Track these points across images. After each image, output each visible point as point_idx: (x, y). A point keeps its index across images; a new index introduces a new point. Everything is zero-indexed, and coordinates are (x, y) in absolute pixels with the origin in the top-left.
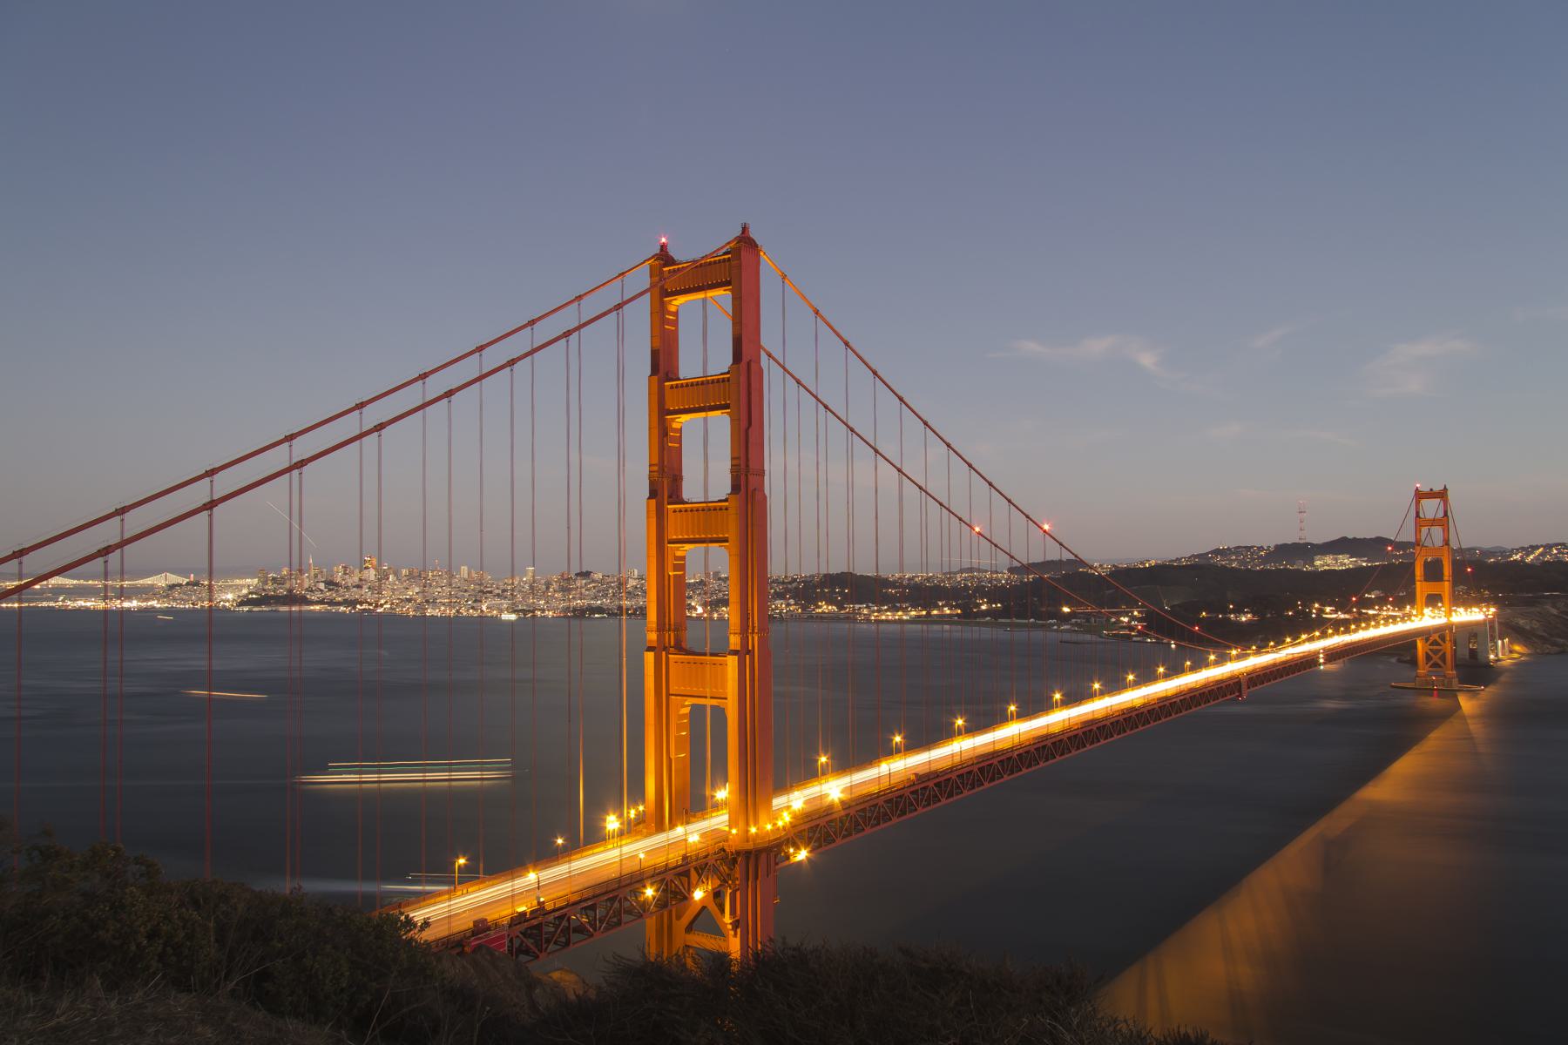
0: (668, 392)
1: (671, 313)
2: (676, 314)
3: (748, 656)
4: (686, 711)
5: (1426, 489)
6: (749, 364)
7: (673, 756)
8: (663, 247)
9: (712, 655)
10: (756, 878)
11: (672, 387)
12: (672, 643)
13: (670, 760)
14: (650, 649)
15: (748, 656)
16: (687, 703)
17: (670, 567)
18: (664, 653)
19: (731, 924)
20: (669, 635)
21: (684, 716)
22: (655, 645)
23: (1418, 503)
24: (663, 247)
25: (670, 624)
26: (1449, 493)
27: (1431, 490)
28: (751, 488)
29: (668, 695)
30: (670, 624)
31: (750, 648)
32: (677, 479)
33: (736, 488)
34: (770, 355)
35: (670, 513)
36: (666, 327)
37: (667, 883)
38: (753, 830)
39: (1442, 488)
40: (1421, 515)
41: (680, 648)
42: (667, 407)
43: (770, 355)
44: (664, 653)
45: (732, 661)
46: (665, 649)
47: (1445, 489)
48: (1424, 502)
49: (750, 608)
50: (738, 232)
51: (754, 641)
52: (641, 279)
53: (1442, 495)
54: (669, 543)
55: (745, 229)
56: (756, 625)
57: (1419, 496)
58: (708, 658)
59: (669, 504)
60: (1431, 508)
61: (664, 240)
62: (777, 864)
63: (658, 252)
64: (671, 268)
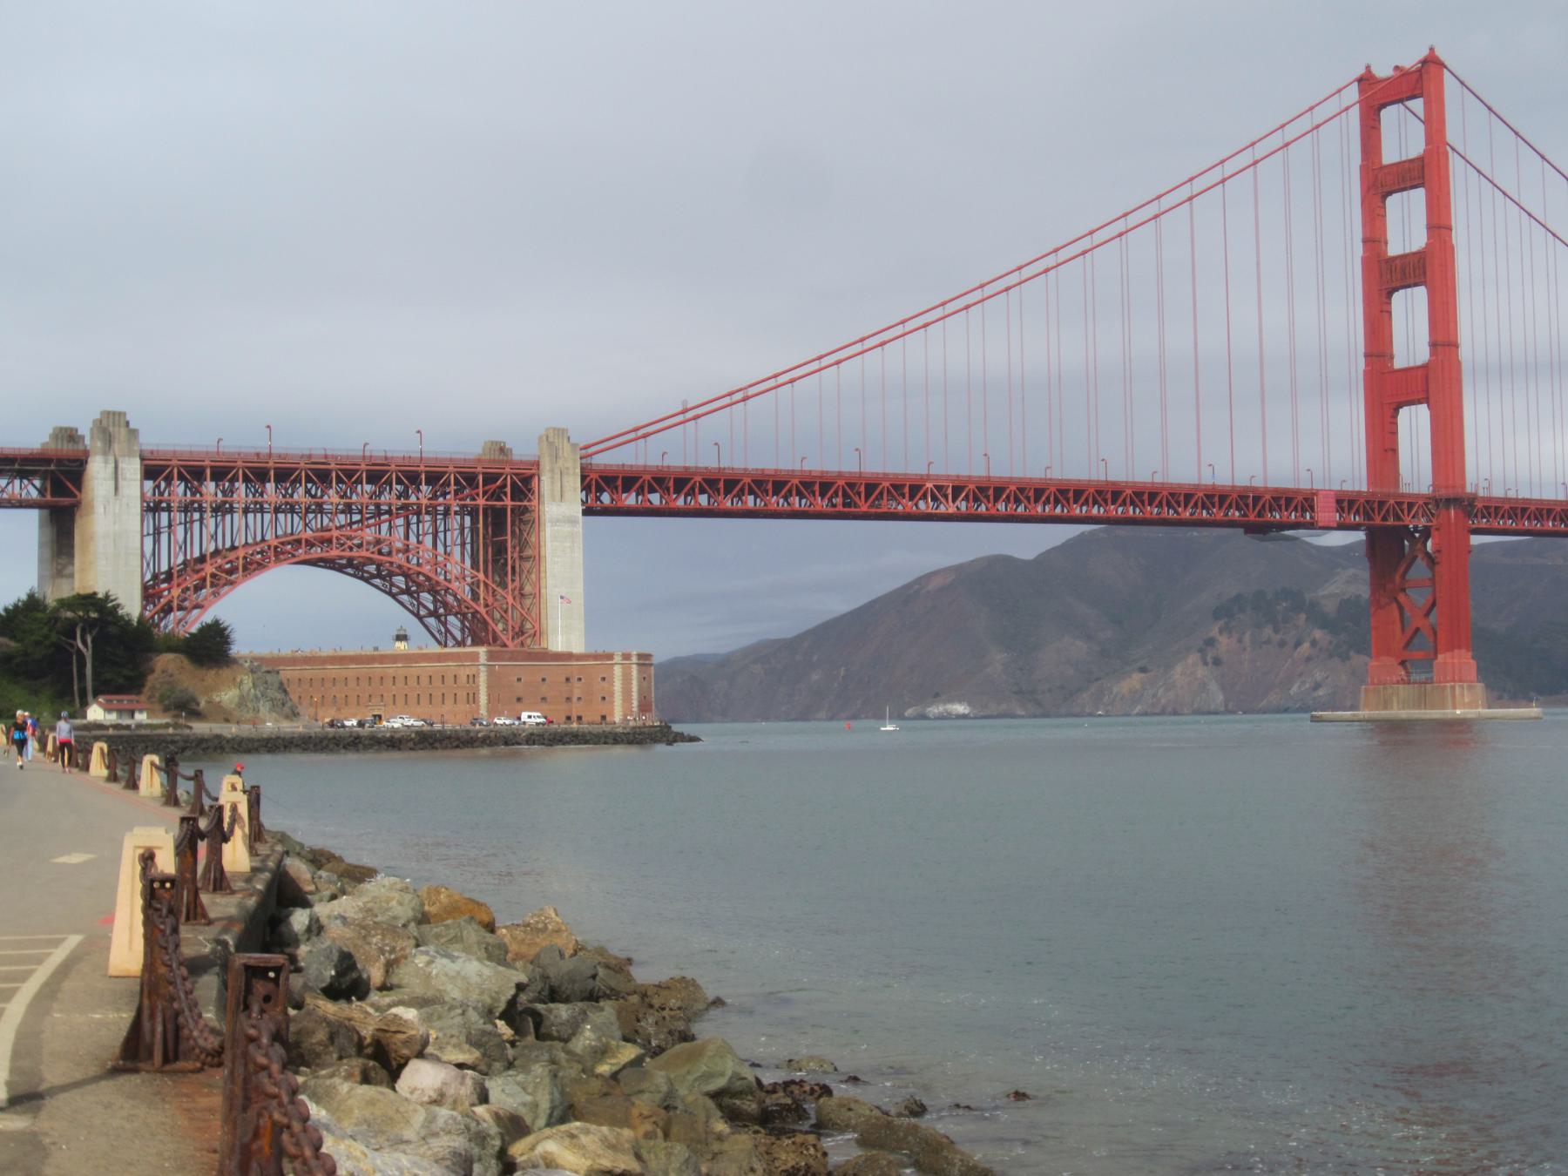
24: (1368, 67)
34: (1453, 149)
43: (1453, 149)
52: (1353, 94)
55: (1432, 49)
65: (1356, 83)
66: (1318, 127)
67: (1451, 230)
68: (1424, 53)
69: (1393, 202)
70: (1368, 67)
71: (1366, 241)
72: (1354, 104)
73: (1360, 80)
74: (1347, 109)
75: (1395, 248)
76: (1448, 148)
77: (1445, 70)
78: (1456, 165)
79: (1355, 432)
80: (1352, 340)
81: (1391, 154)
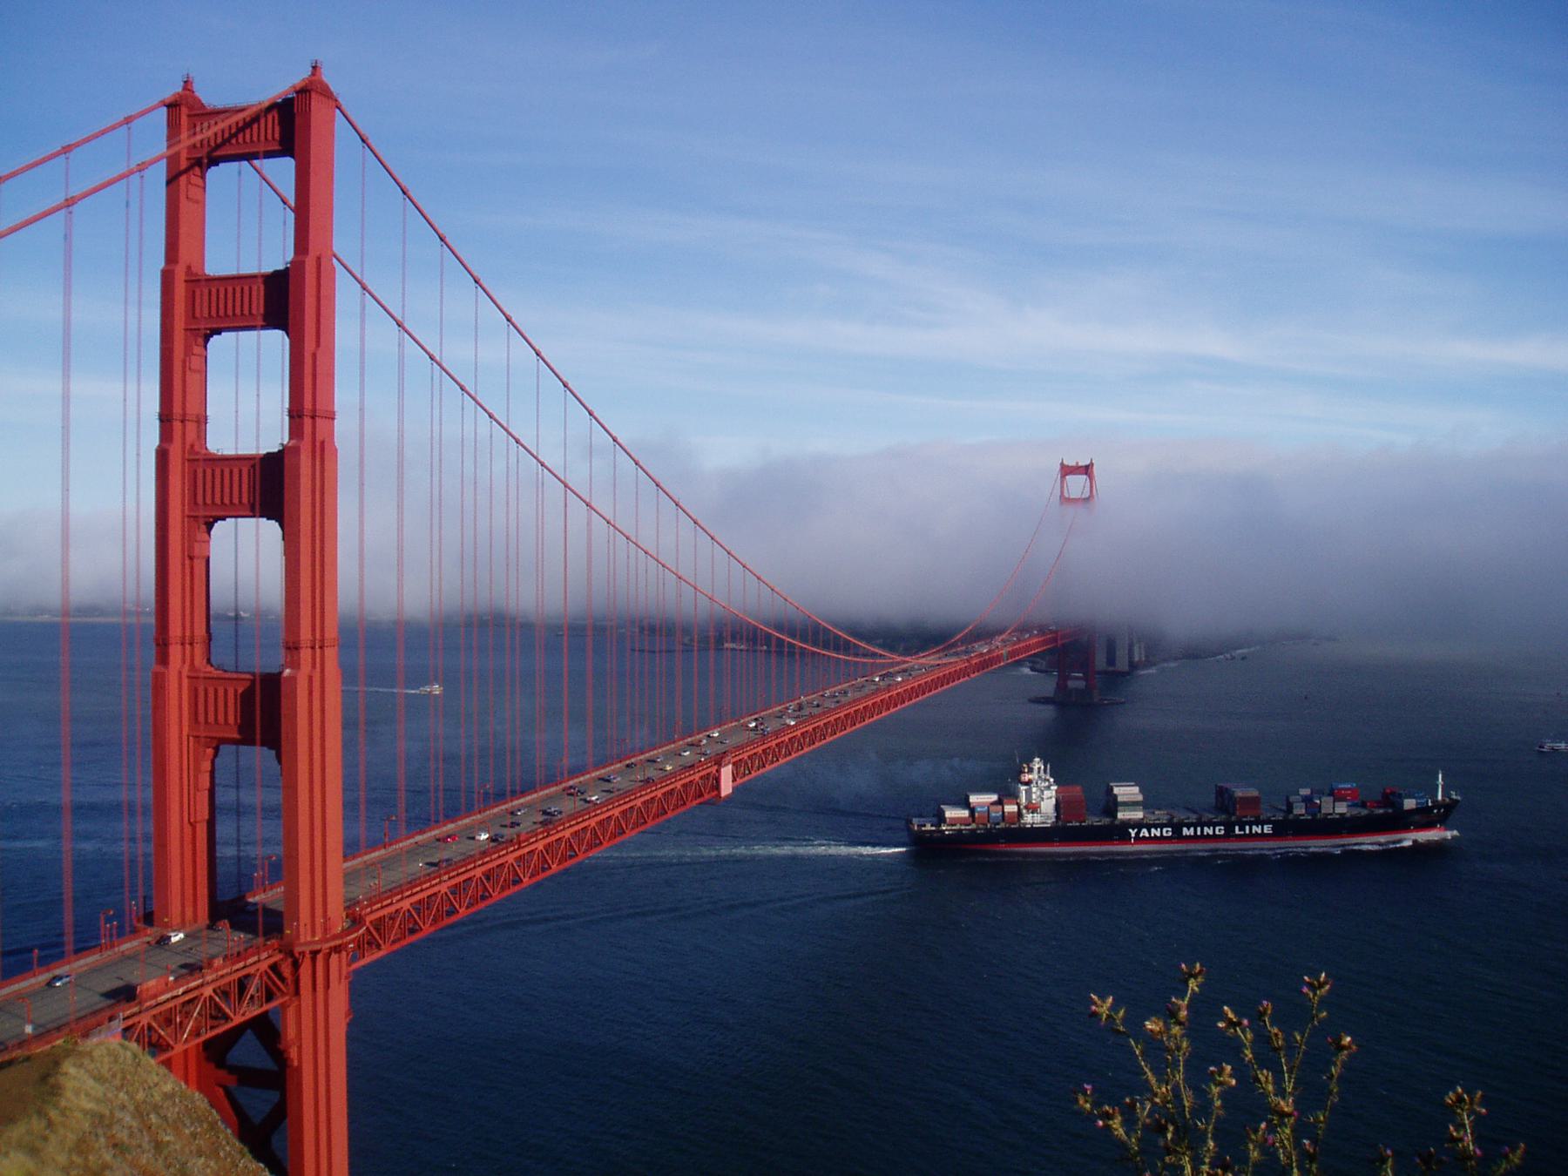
5: (1074, 464)
6: (319, 259)
10: (327, 986)
23: (1063, 476)
24: (187, 84)
26: (1095, 467)
27: (1077, 463)
28: (319, 438)
32: (202, 420)
33: (296, 431)
37: (205, 1001)
39: (1088, 463)
40: (1066, 495)
47: (1092, 464)
48: (1067, 477)
50: (306, 73)
53: (1087, 470)
57: (1066, 470)
60: (1077, 484)
62: (349, 965)
63: (180, 90)
65: (165, 109)
66: (70, 203)
67: (333, 419)
68: (300, 75)
69: (222, 346)
70: (187, 84)
71: (166, 418)
72: (159, 159)
73: (173, 106)
74: (142, 167)
75: (225, 437)
76: (335, 260)
77: (338, 111)
78: (345, 295)
79: (131, 486)
80: (131, 505)
81: (221, 260)
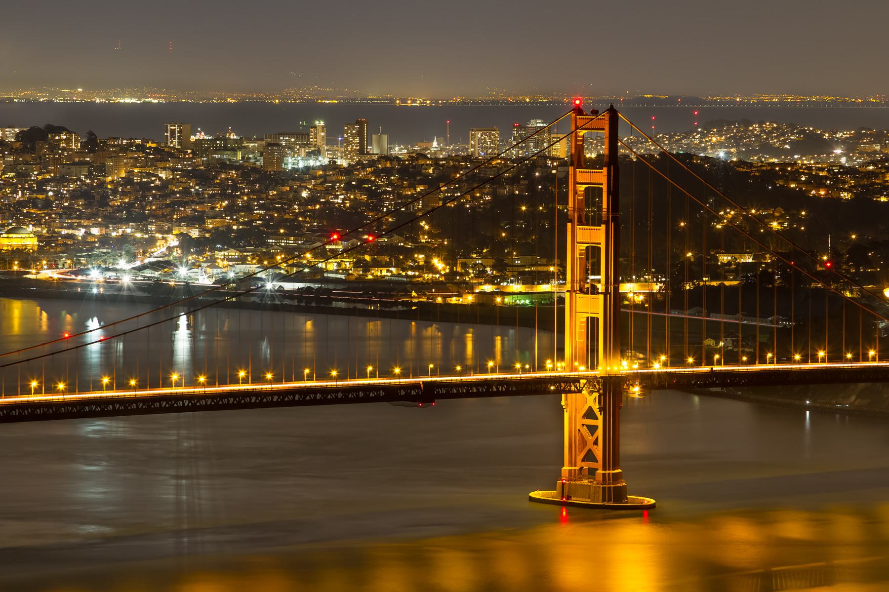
0: (578, 173)
1: (579, 137)
2: (583, 136)
3: (608, 295)
4: (585, 320)
7: (578, 340)
8: (578, 106)
9: (591, 294)
11: (580, 172)
12: (578, 289)
13: (576, 342)
14: (568, 291)
15: (608, 295)
16: (584, 316)
17: (578, 254)
18: (574, 293)
19: (599, 408)
20: (577, 285)
21: (582, 322)
22: (570, 290)
25: (577, 281)
29: (576, 312)
30: (577, 281)
31: (610, 292)
35: (578, 230)
36: (578, 143)
38: (608, 369)
41: (581, 291)
42: (577, 180)
44: (574, 293)
45: (601, 297)
46: (575, 291)
49: (610, 276)
51: (611, 288)
54: (577, 243)
55: (612, 106)
56: (612, 281)
58: (589, 296)
59: (577, 225)
61: (578, 102)
64: (581, 117)
